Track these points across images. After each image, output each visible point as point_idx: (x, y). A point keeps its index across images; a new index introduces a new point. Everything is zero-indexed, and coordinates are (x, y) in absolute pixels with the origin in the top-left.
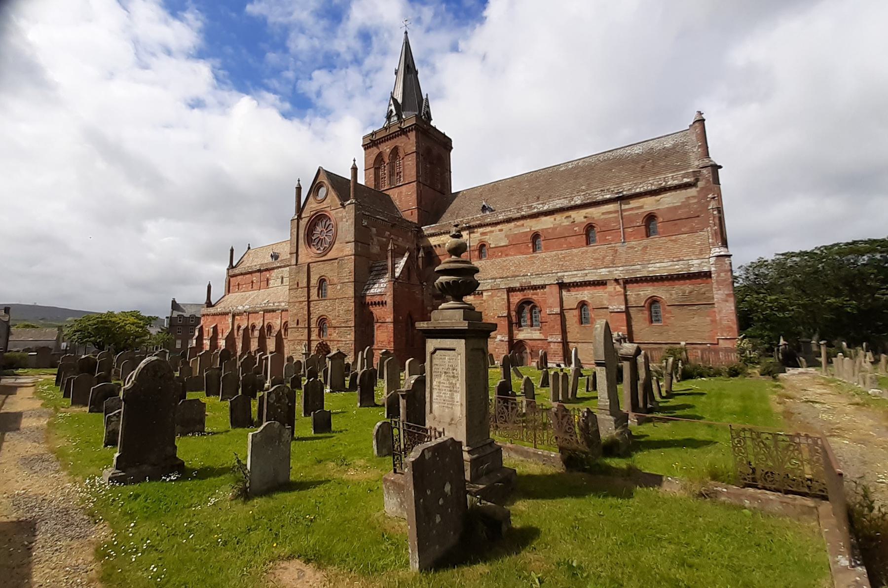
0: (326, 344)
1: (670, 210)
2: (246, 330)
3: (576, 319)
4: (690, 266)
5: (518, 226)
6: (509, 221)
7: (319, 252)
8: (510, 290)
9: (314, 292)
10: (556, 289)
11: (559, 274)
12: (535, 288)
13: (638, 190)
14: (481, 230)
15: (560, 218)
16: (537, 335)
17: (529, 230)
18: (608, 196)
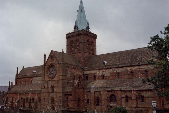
0: (54, 106)
1: (151, 70)
2: (25, 99)
3: (124, 101)
4: (150, 88)
5: (113, 70)
6: (110, 68)
7: (51, 77)
8: (108, 91)
9: (50, 90)
10: (120, 92)
11: (121, 87)
12: (115, 91)
13: (143, 63)
14: (103, 70)
15: (124, 69)
16: (115, 104)
17: (116, 72)
18: (136, 64)
